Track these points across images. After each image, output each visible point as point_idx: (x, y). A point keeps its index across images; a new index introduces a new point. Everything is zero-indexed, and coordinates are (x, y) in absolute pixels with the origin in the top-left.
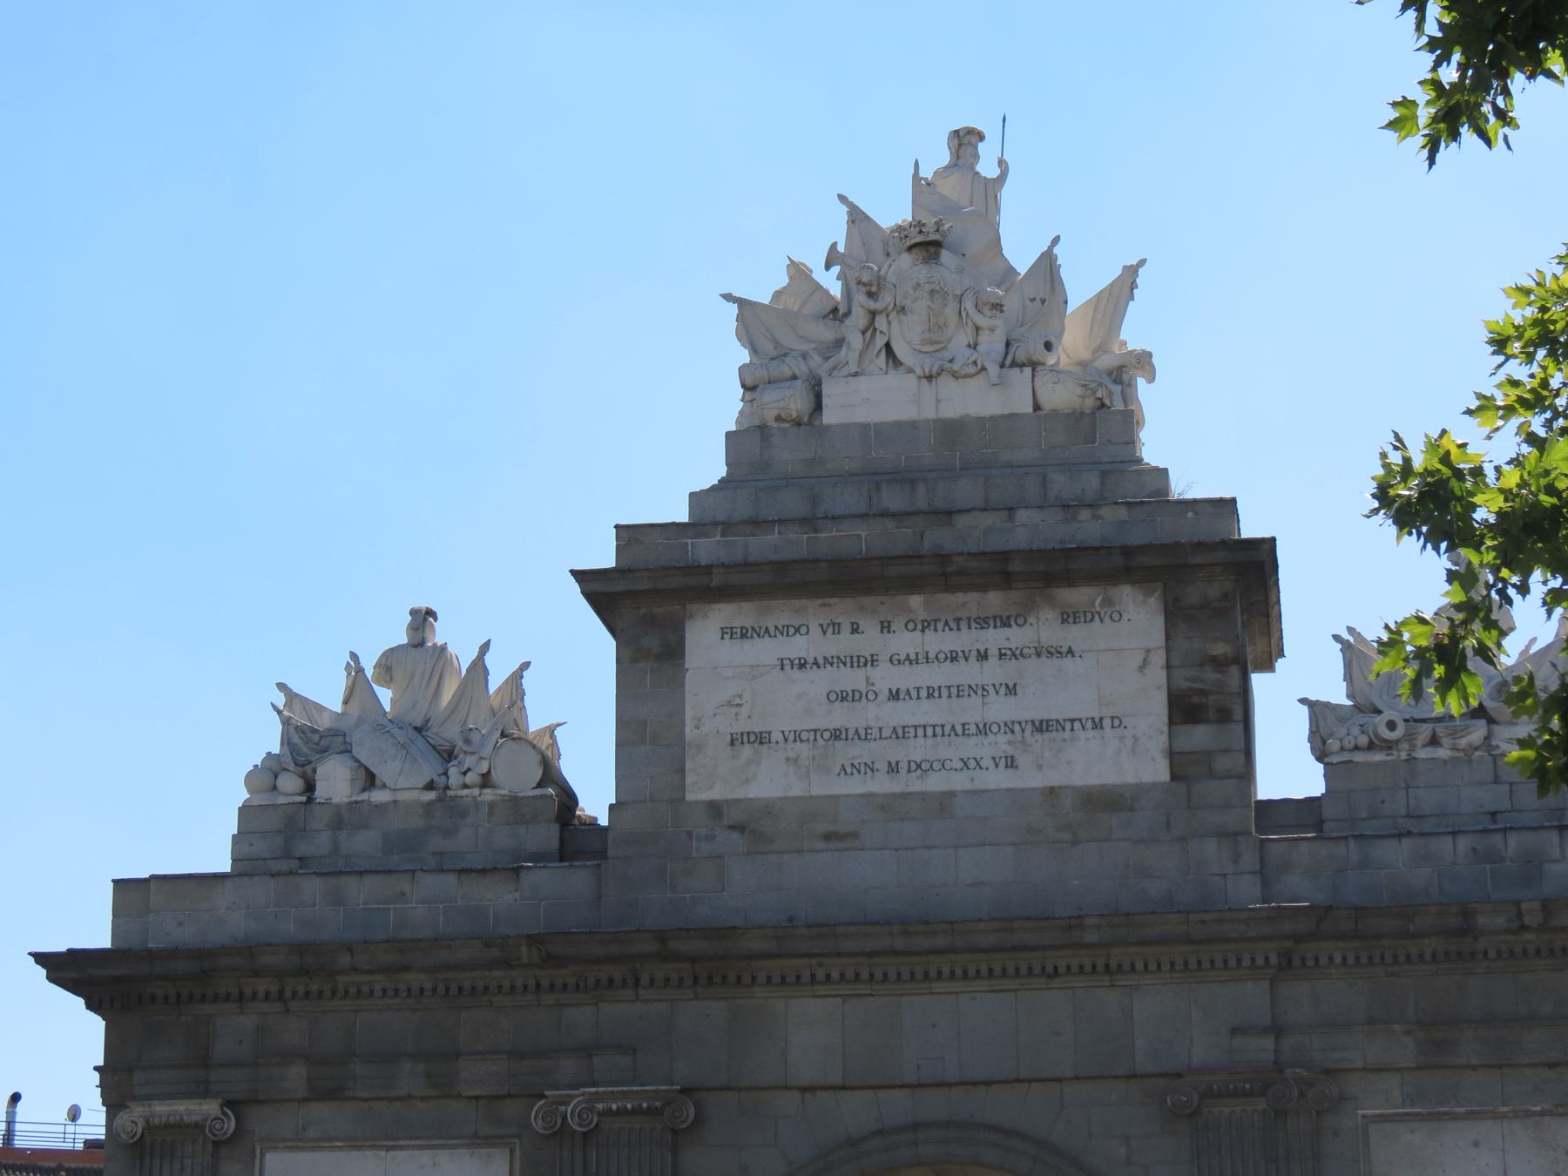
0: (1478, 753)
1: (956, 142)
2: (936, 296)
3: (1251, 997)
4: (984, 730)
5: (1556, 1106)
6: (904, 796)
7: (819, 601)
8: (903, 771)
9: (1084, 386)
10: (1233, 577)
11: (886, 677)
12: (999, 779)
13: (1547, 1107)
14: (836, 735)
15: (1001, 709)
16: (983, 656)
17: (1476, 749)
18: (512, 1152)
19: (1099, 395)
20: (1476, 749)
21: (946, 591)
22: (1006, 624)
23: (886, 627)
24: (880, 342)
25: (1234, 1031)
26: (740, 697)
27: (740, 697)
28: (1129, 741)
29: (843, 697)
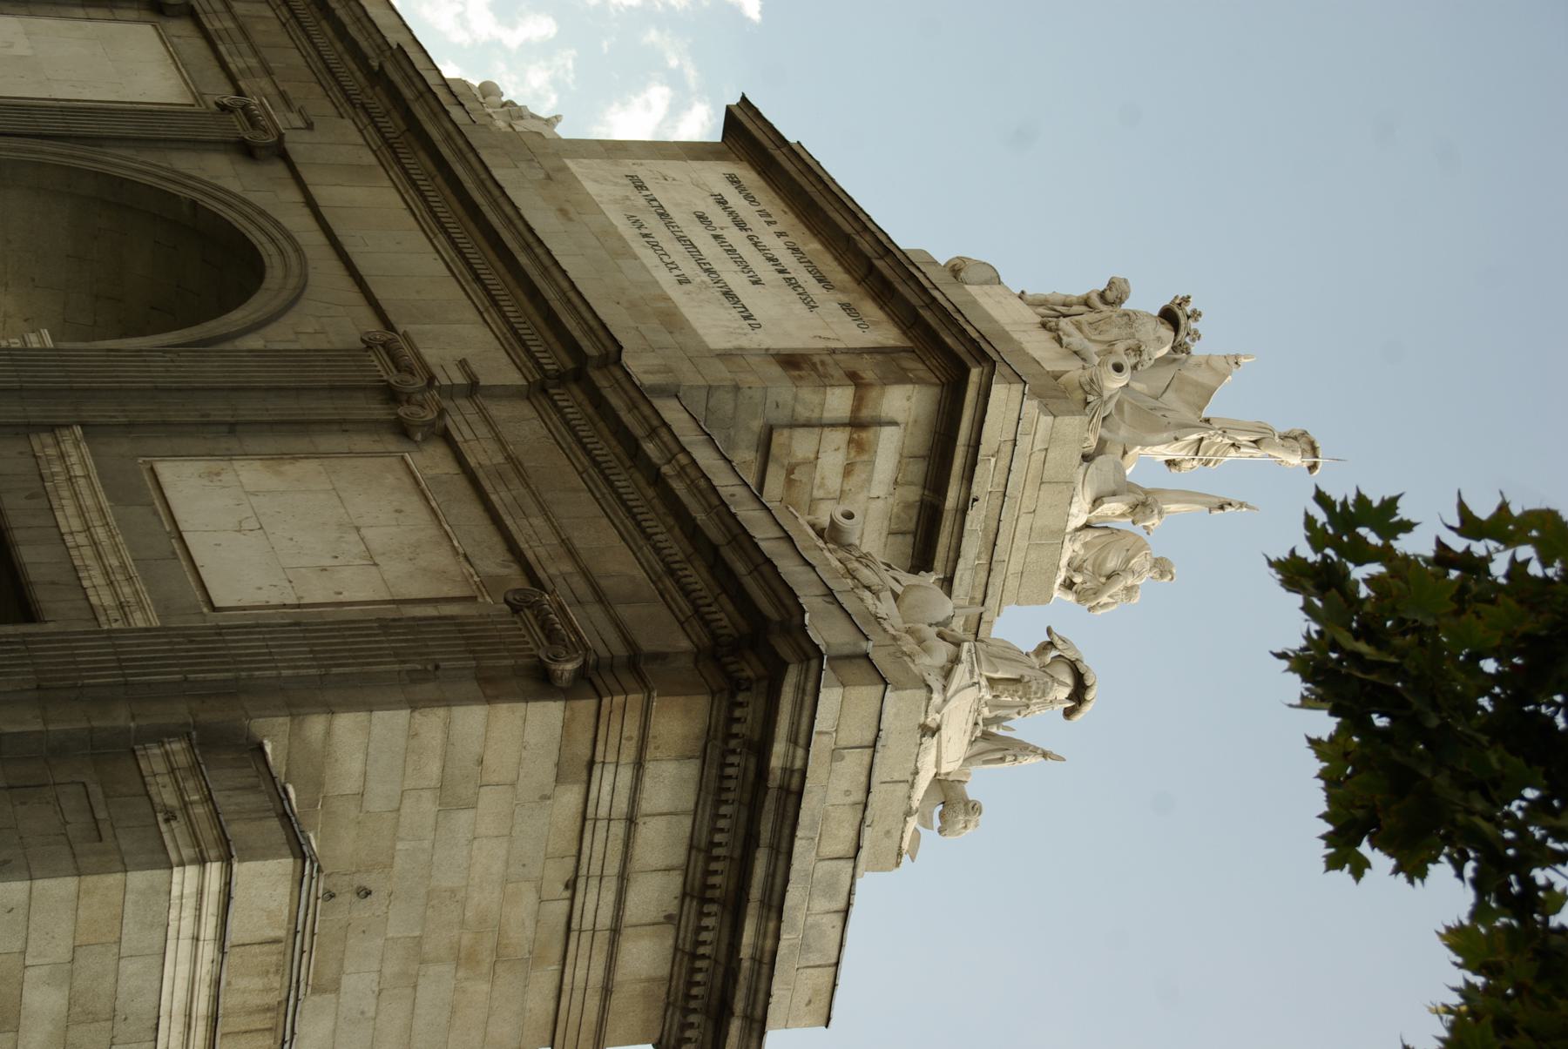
0: (849, 581)
1: (1296, 433)
2: (1125, 318)
3: (500, 370)
4: (709, 271)
5: (466, 556)
6: (621, 238)
7: (786, 209)
8: (646, 239)
9: (1092, 380)
10: (943, 380)
11: (734, 236)
12: (666, 279)
13: (461, 550)
14: (663, 215)
15: (736, 281)
16: (781, 272)
17: (854, 578)
18: (193, 105)
19: (1090, 398)
20: (854, 578)
21: (836, 259)
22: (820, 281)
23: (780, 234)
24: (1064, 310)
25: (463, 364)
26: (674, 180)
27: (674, 180)
28: (740, 331)
29: (702, 218)
